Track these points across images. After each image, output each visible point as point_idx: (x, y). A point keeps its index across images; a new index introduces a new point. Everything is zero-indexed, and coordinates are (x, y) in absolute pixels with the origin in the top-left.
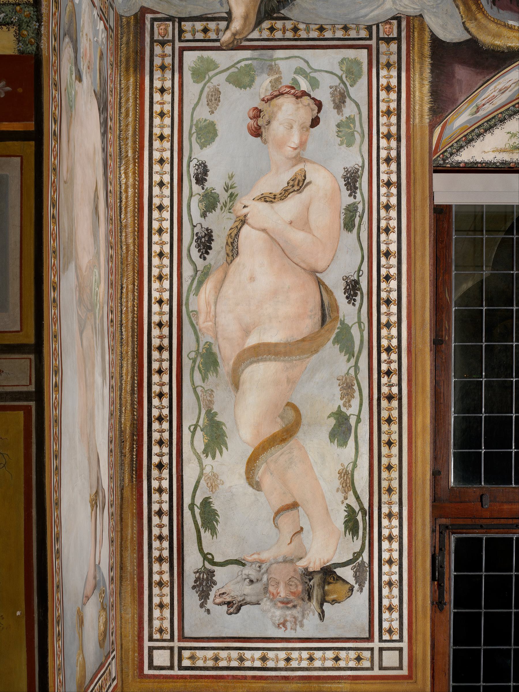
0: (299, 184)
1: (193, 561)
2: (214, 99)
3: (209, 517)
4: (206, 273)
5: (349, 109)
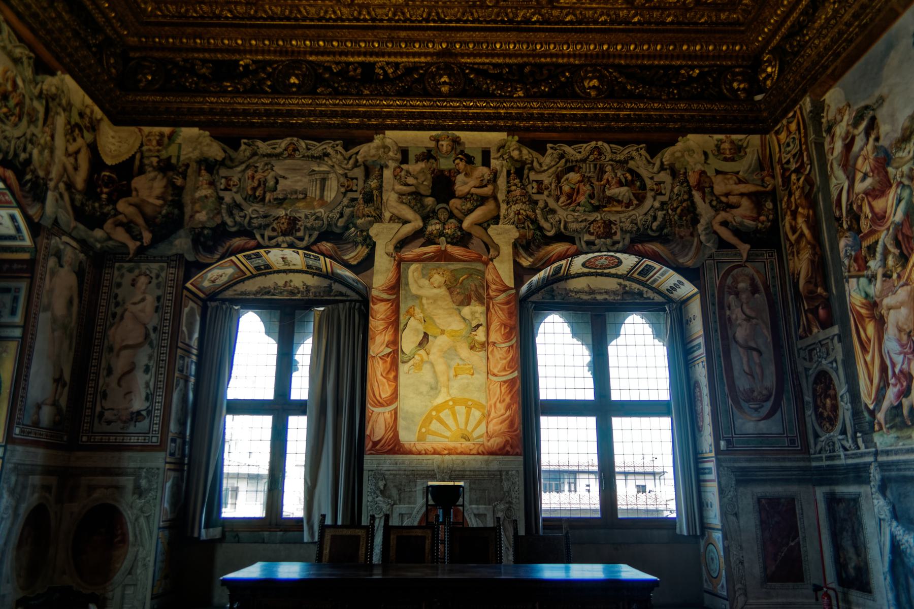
0: (143, 300)
1: (98, 409)
2: (122, 276)
3: (105, 396)
4: (114, 324)
5: (160, 279)
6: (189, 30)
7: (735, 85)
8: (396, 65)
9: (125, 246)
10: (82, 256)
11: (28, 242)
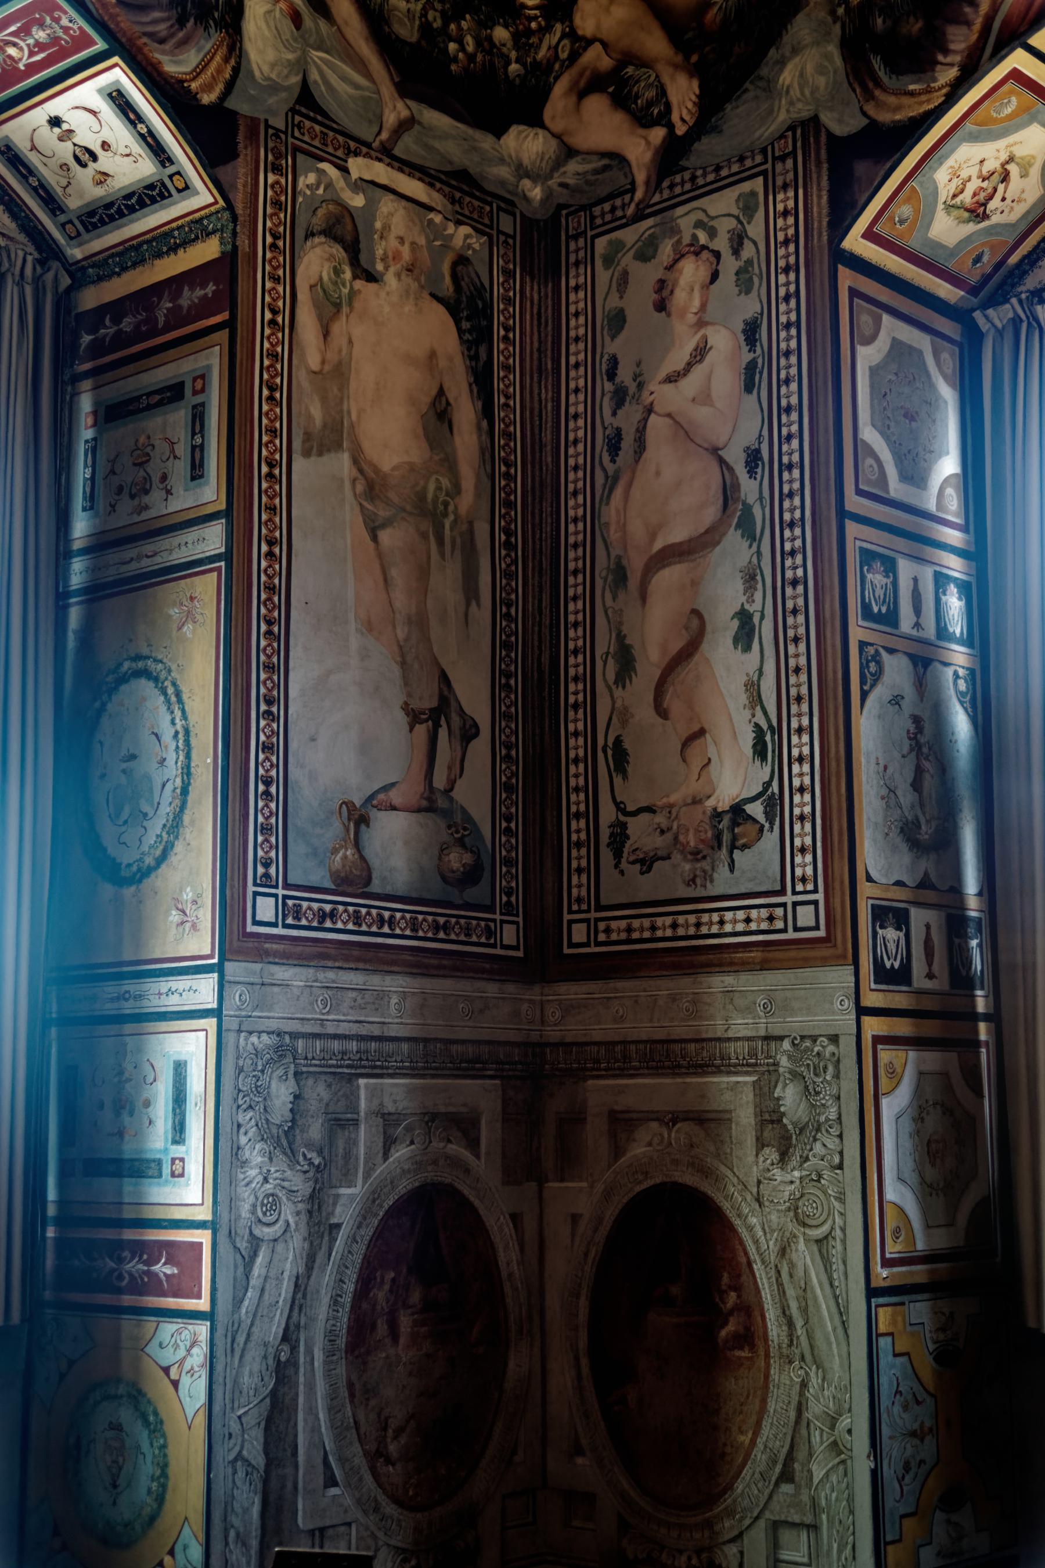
0: (701, 352)
1: (607, 814)
2: (623, 281)
3: (620, 758)
4: (616, 479)
5: (748, 251)
9: (616, 159)
10: (461, 235)
11: (202, 196)
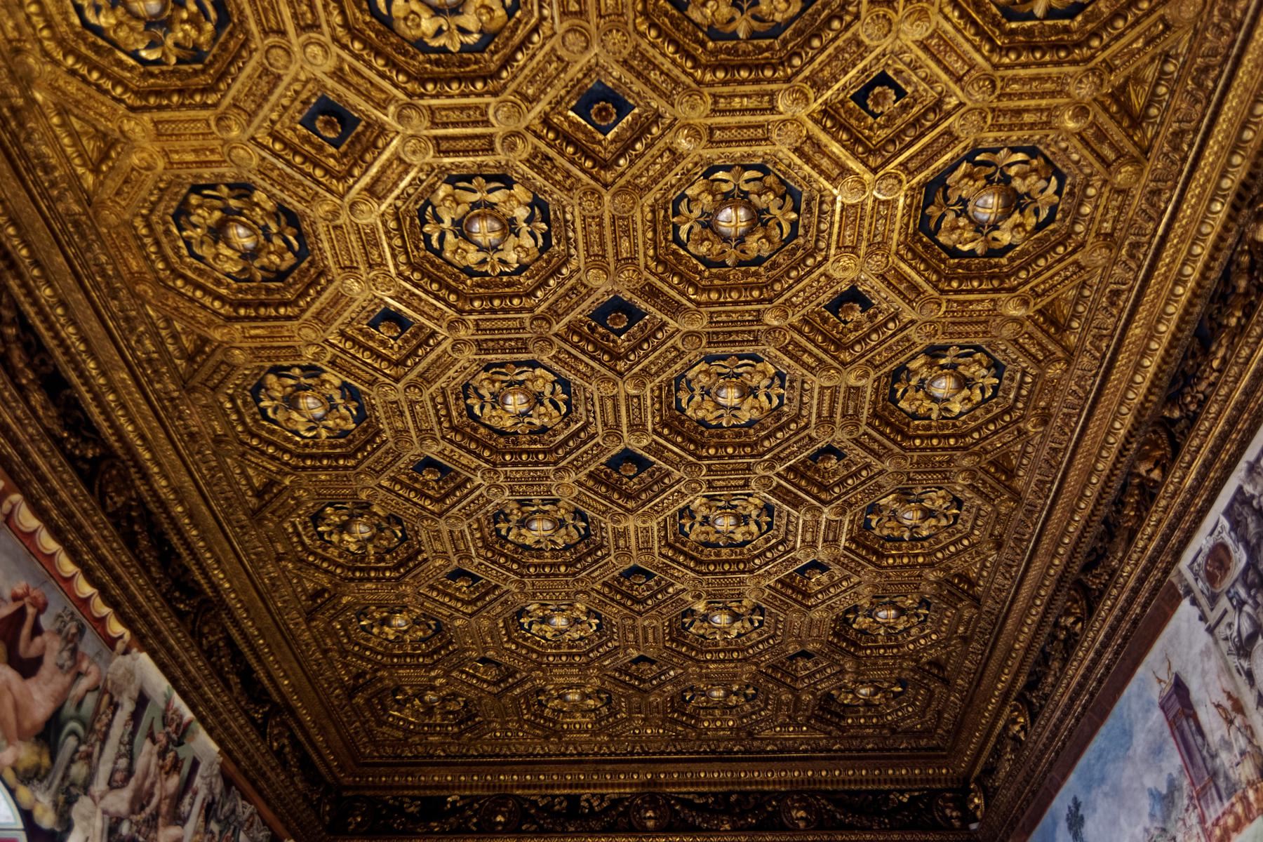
6: (403, 769)
7: (948, 811)
8: (603, 796)
